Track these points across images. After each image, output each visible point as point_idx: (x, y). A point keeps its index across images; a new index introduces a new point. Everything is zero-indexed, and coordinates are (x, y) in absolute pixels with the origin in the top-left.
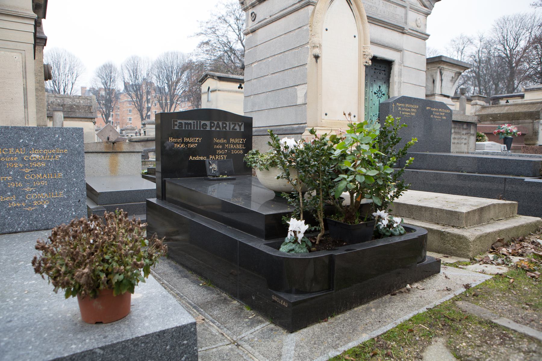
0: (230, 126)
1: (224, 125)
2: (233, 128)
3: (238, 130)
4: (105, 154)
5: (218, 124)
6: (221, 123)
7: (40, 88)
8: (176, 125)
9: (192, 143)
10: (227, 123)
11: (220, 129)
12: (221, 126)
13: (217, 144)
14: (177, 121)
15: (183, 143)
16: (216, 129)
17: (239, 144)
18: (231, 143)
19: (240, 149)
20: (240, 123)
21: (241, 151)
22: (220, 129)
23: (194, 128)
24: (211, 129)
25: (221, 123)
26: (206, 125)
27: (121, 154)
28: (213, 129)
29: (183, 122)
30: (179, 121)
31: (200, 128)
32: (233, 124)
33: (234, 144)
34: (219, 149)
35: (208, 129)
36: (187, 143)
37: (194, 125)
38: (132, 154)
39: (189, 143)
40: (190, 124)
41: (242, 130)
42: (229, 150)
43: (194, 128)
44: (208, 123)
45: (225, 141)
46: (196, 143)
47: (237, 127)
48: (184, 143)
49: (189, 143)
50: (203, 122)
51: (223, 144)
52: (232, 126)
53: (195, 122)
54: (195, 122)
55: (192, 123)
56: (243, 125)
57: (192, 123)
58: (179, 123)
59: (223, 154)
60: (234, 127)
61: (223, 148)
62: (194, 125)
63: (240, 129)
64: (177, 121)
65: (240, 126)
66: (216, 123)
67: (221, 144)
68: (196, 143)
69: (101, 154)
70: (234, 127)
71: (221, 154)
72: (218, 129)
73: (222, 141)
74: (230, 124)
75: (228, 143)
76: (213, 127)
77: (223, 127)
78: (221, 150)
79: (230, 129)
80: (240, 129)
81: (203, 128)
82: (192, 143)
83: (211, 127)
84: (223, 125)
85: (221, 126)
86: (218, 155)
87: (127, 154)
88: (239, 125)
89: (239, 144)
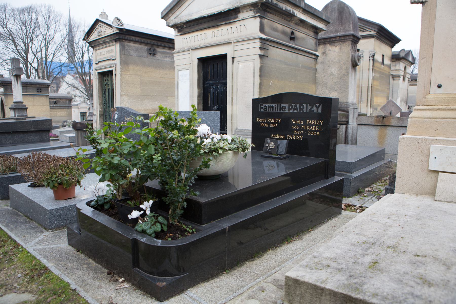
0: (306, 108)
1: (302, 107)
2: (310, 110)
3: (315, 111)
4: (375, 127)
5: (296, 106)
6: (298, 105)
7: (346, 74)
8: (262, 108)
9: (273, 123)
10: (305, 105)
11: (297, 111)
12: (298, 108)
13: (294, 125)
14: (263, 105)
15: (266, 123)
16: (293, 111)
17: (316, 126)
18: (308, 125)
19: (316, 131)
20: (317, 105)
21: (318, 133)
22: (297, 111)
23: (275, 110)
24: (289, 110)
25: (298, 105)
26: (285, 108)
27: (390, 128)
28: (291, 111)
29: (267, 105)
30: (264, 105)
31: (280, 110)
32: (310, 105)
33: (310, 125)
34: (296, 130)
35: (287, 111)
36: (270, 123)
37: (275, 107)
38: (401, 128)
39: (272, 123)
40: (273, 106)
41: (320, 111)
42: (307, 131)
43: (275, 110)
44: (286, 105)
45: (302, 123)
46: (276, 123)
47: (314, 109)
48: (268, 123)
49: (272, 123)
50: (282, 105)
51: (300, 126)
52: (309, 108)
53: (276, 105)
54: (276, 105)
55: (274, 106)
56: (321, 107)
57: (274, 106)
58: (265, 106)
59: (299, 135)
60: (311, 108)
61: (300, 129)
62: (275, 107)
63: (318, 111)
64: (263, 105)
65: (317, 108)
66: (293, 105)
67: (297, 125)
68: (276, 123)
69: (372, 127)
70: (311, 108)
71: (298, 135)
72: (296, 111)
73: (299, 122)
74: (307, 106)
75: (305, 124)
76: (291, 109)
77: (300, 109)
78: (298, 130)
79: (307, 111)
80: (318, 111)
81: (282, 110)
82: (273, 123)
83: (289, 109)
84: (300, 107)
85: (298, 108)
86: (295, 135)
87: (395, 128)
88: (316, 106)
89: (316, 126)
